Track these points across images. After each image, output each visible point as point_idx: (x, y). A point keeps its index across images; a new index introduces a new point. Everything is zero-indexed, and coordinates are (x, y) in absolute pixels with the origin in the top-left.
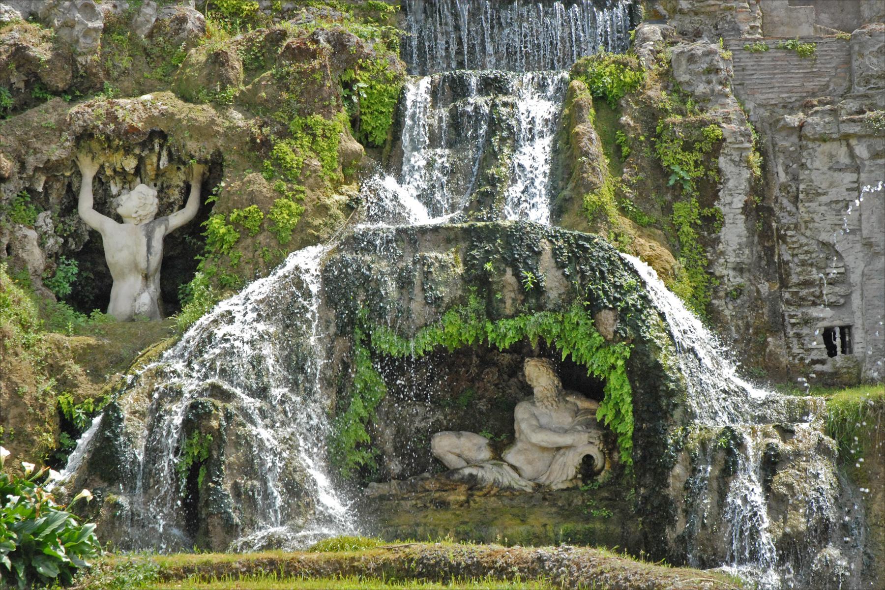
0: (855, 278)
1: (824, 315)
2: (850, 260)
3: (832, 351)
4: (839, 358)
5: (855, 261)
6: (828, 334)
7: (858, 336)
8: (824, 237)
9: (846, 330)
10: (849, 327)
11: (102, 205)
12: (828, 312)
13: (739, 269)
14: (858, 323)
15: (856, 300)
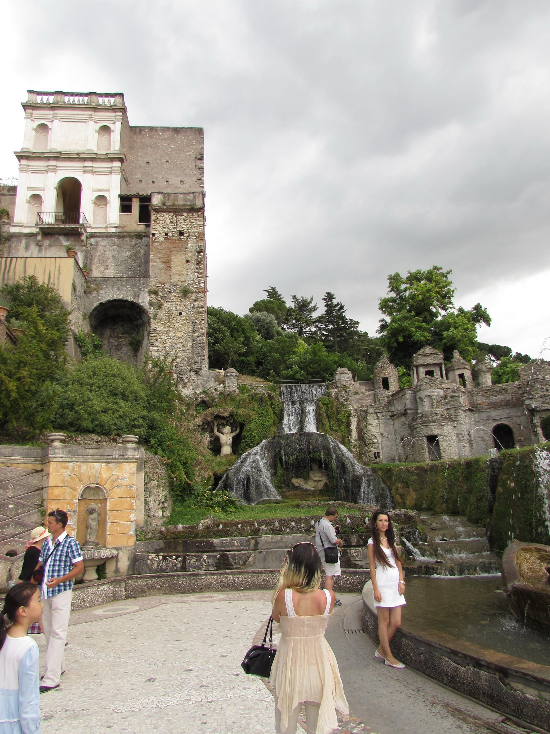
0: (380, 442)
1: (374, 450)
2: (378, 438)
3: (376, 458)
4: (378, 459)
5: (379, 438)
6: (375, 454)
7: (381, 454)
8: (373, 433)
9: (378, 453)
10: (378, 453)
11: (218, 431)
12: (374, 450)
13: (356, 441)
14: (381, 452)
15: (380, 447)
